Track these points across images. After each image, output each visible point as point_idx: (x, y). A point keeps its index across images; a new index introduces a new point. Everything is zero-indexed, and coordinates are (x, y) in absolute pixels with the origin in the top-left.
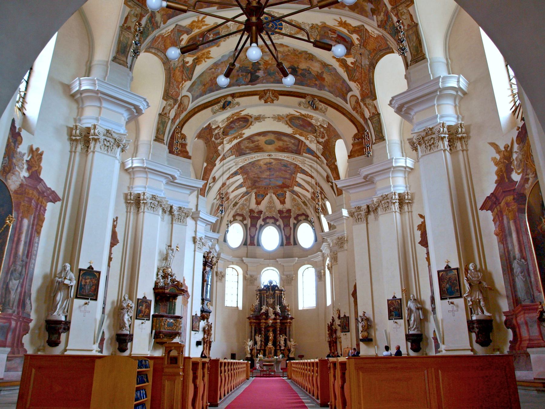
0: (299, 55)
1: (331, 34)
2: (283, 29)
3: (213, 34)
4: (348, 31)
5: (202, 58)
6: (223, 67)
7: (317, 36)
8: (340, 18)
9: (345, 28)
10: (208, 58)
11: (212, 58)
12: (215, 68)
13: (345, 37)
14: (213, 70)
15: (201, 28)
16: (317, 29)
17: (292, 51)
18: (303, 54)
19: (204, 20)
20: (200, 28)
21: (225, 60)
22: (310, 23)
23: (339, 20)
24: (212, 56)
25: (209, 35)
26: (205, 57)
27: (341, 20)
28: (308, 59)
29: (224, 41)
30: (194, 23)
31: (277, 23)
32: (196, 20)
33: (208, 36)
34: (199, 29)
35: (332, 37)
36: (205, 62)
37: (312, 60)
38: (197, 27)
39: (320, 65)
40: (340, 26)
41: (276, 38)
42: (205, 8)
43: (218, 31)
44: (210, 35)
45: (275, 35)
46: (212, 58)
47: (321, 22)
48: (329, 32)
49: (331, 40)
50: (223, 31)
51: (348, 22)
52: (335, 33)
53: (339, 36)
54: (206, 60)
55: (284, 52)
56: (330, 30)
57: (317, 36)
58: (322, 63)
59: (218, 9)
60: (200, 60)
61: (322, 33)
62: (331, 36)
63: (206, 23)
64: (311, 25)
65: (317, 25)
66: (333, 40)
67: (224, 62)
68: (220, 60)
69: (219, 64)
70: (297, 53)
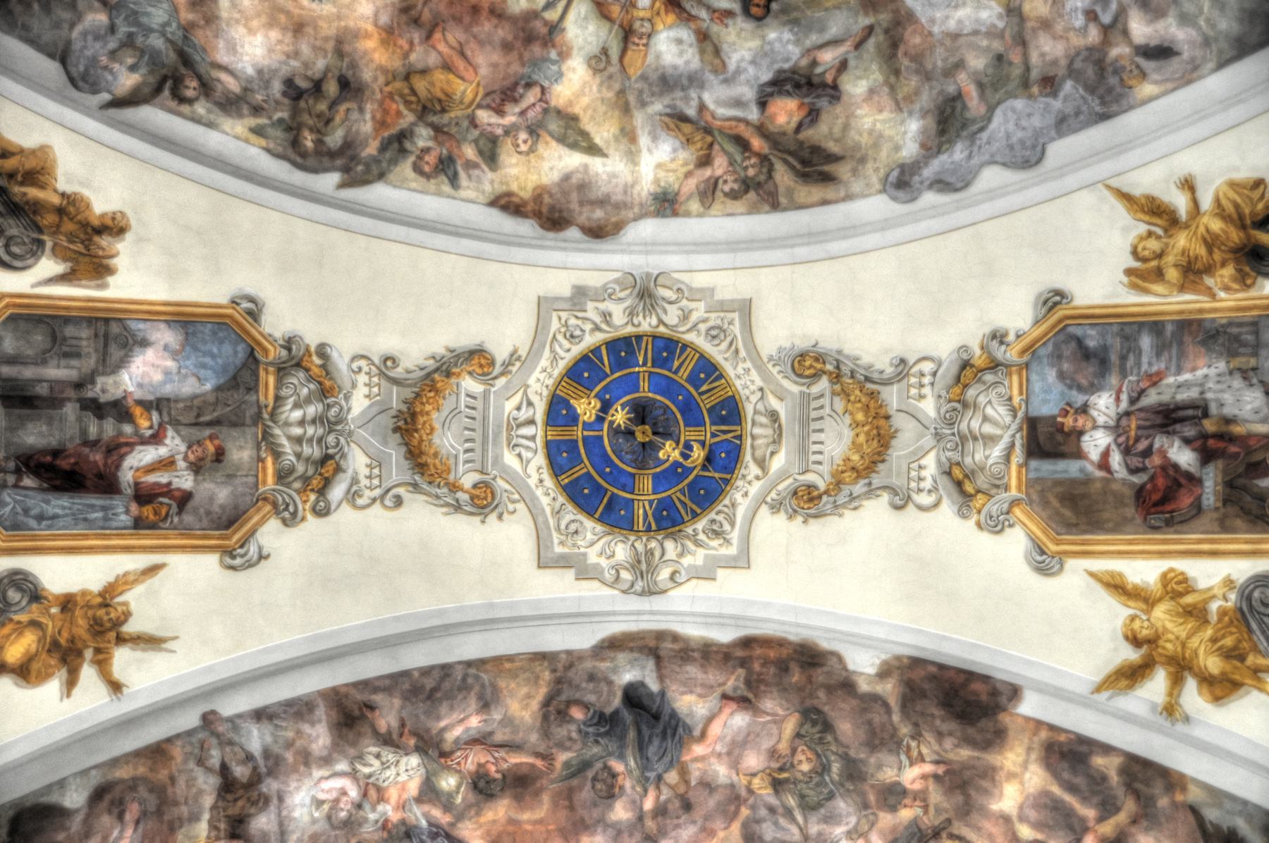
0: (409, 118)
1: (167, 464)
2: (540, 412)
3: (1079, 454)
4: (36, 595)
5: (1211, 242)
6: (1046, 24)
7: (278, 399)
8: (116, 687)
9: (68, 603)
10: (1153, 209)
11: (1126, 197)
12: (1119, 51)
13: (60, 504)
14: (1140, 29)
15: (1165, 578)
16: (283, 476)
17: (469, 152)
18: (371, 149)
19: (1131, 655)
20: (1175, 587)
21: (1019, 104)
22: (345, 516)
23: (122, 659)
24: (1120, 208)
25: (1116, 459)
26: (1182, 240)
27: (102, 664)
28: (332, 88)
29: (998, 336)
30: (1213, 664)
31: (586, 467)
32: (1191, 684)
33: (1126, 451)
34: (1184, 580)
35: (156, 438)
36: (1188, 185)
37: (293, 92)
38: (1196, 613)
39: (222, 57)
40: (108, 594)
41: (592, 311)
42: (1107, 749)
43: (1034, 464)
44: (1104, 464)
45: (599, 337)
46: (1126, 197)
47: (262, 557)
48: (185, 481)
49: (158, 404)
50: (997, 452)
51: (53, 686)
52: (144, 496)
53: (107, 484)
54: (1181, 203)
55: (534, 131)
56: (184, 499)
57: (278, 399)
58: (206, 88)
59: (1015, 692)
60: (1235, 236)
61: (241, 453)
62: (173, 444)
63: (1117, 613)
64: (337, 492)
65: (291, 519)
66: (146, 405)
67: (1025, 84)
68: (1063, 125)
69: (1072, 73)
70: (423, 137)
